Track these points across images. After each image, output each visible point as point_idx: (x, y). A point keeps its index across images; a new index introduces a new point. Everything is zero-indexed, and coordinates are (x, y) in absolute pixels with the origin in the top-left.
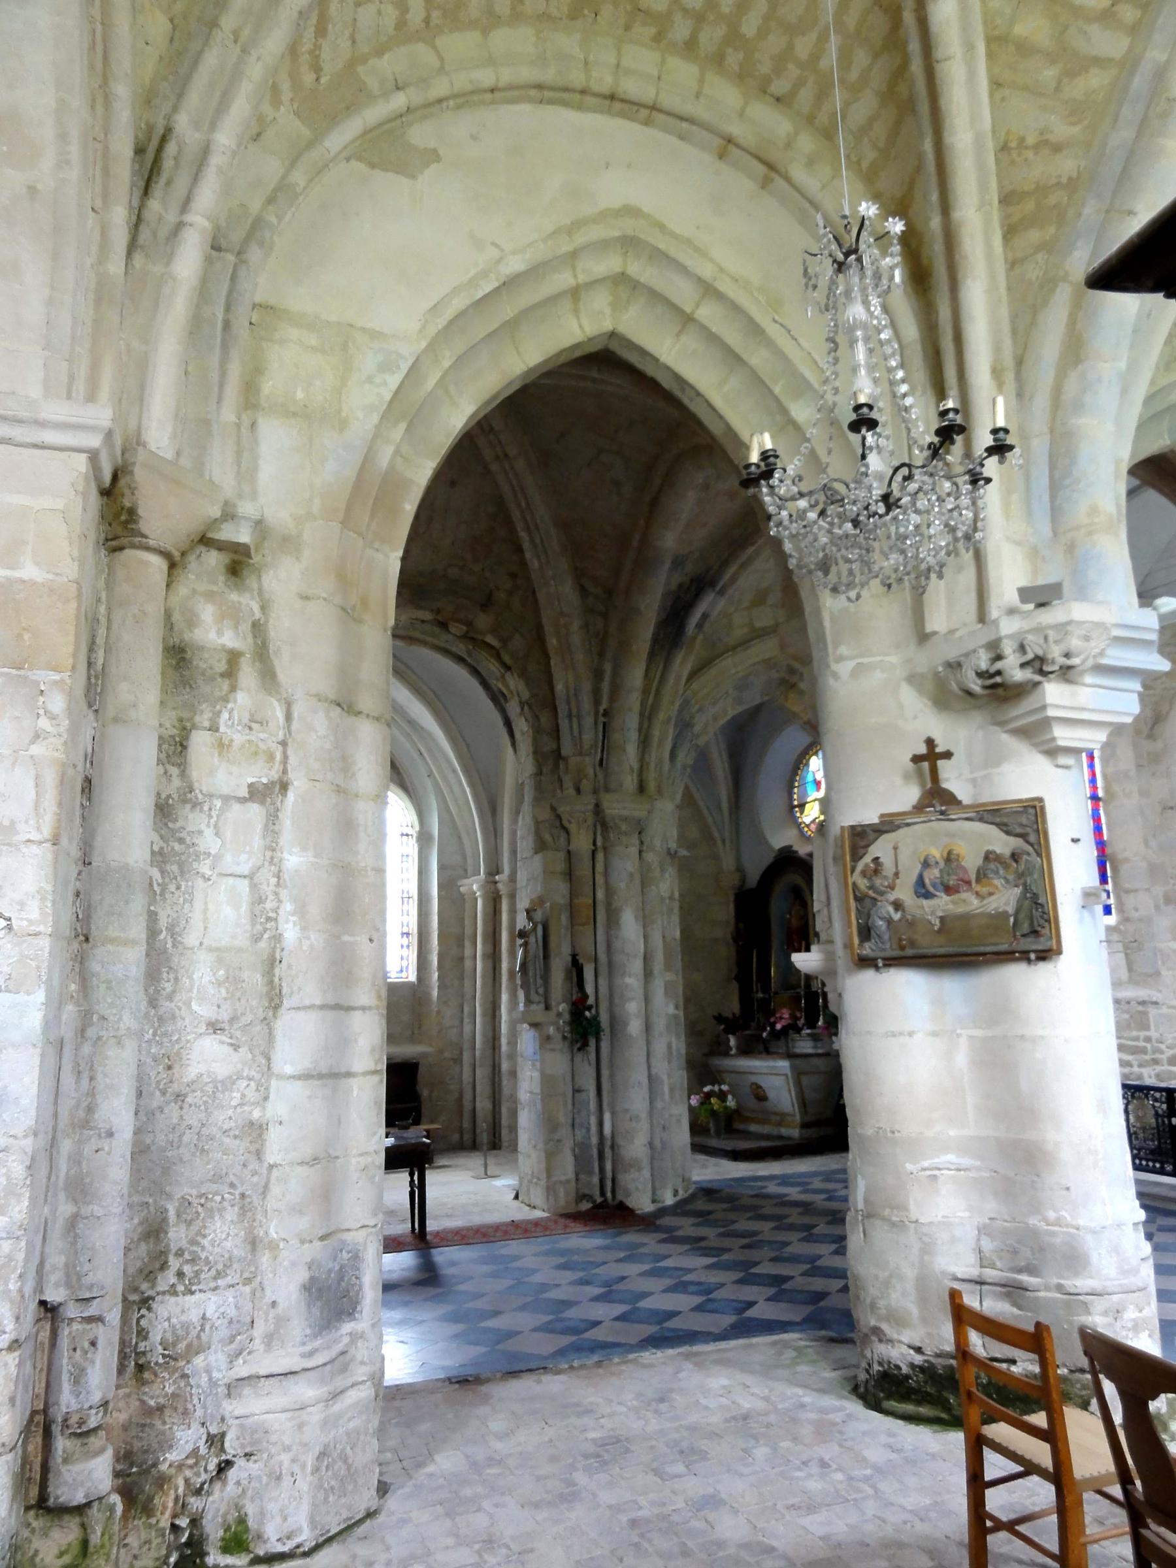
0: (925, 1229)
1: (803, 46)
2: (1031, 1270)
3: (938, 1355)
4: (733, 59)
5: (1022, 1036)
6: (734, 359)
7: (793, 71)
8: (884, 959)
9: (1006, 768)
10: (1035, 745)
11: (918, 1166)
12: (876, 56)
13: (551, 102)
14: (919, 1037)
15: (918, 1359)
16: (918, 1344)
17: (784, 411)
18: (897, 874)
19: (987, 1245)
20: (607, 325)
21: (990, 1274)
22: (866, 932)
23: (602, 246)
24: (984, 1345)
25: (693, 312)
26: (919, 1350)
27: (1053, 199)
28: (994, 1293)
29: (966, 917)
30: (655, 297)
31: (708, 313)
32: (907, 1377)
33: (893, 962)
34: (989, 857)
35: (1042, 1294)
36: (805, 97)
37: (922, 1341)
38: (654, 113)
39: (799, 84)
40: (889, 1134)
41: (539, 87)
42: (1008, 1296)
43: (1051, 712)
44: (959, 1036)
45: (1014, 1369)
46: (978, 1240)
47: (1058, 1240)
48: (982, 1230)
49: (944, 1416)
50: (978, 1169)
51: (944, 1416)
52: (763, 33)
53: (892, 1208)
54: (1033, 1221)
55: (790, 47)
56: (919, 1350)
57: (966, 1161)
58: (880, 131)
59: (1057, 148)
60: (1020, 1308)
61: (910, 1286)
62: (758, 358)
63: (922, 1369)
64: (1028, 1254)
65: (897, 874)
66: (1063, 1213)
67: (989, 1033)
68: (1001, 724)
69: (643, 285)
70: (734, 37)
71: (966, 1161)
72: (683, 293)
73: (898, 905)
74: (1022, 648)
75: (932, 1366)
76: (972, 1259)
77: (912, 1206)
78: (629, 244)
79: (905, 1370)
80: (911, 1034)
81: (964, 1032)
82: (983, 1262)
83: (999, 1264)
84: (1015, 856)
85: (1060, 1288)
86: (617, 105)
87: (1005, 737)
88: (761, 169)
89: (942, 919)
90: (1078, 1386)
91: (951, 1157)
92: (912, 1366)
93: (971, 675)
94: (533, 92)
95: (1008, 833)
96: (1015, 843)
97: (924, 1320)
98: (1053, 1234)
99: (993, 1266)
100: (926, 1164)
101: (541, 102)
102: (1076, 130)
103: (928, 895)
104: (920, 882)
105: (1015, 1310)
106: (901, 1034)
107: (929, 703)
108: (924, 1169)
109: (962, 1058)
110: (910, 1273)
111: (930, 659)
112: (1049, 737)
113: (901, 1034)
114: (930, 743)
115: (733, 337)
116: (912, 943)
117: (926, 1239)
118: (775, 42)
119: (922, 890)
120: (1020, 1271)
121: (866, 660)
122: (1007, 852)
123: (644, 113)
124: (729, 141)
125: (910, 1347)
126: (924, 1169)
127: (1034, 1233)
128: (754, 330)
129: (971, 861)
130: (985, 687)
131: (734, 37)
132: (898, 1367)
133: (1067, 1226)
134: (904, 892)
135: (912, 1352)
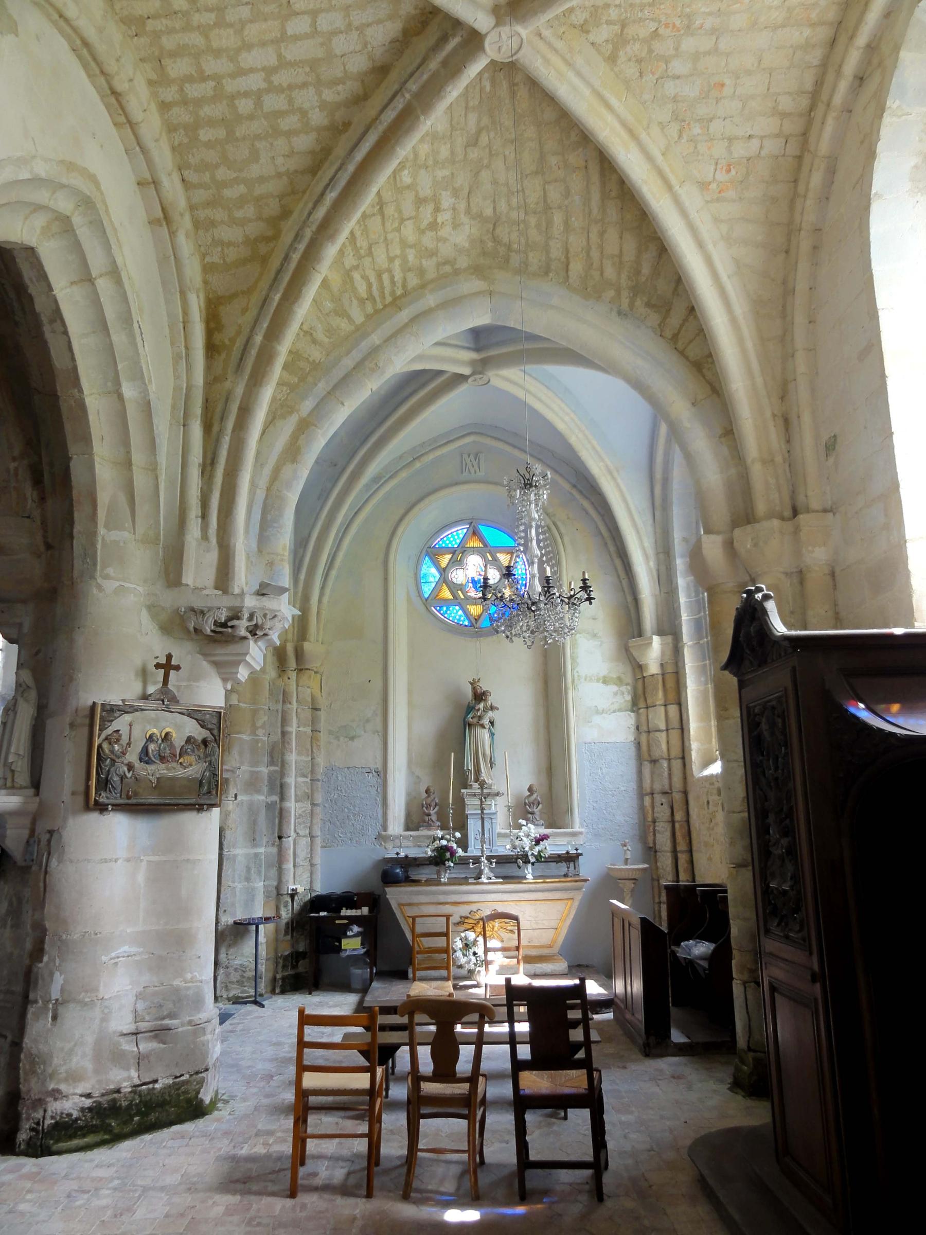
0: (106, 1003)
1: (222, 173)
2: (171, 1016)
3: (103, 1095)
4: (180, 137)
5: (188, 860)
6: (103, 326)
7: (207, 177)
8: (113, 805)
9: (203, 684)
10: (219, 673)
11: (109, 957)
12: (260, 218)
13: (80, 57)
14: (120, 862)
15: (88, 1103)
16: (88, 1092)
17: (118, 383)
18: (129, 744)
19: (140, 1006)
20: (33, 242)
21: (143, 1026)
22: (104, 784)
23: (75, 192)
24: (139, 1076)
25: (95, 279)
26: (88, 1096)
27: (302, 364)
28: (145, 1038)
29: (173, 779)
30: (77, 247)
31: (104, 285)
32: (77, 1119)
33: (118, 808)
34: (189, 740)
35: (180, 1030)
36: (201, 195)
37: (93, 1087)
38: (128, 125)
39: (201, 186)
40: (93, 936)
41: (86, 44)
42: (156, 1037)
43: (248, 658)
44: (141, 861)
45: (157, 1086)
46: (135, 1004)
47: (191, 992)
48: (139, 996)
49: (106, 1137)
50: (140, 954)
51: (106, 1137)
52: (209, 145)
53: (87, 991)
54: (177, 982)
55: (217, 166)
56: (88, 1096)
57: (134, 950)
58: (232, 254)
59: (314, 341)
60: (165, 1044)
61: (89, 1050)
62: (118, 338)
63: (90, 1109)
64: (171, 1006)
65: (129, 744)
66: (196, 973)
67: (164, 858)
68: (205, 655)
69: (75, 235)
70: (192, 129)
71: (134, 950)
72: (97, 262)
73: (130, 767)
74: (251, 618)
75: (99, 1104)
76: (130, 1018)
77: (101, 988)
78: (87, 203)
79: (75, 1114)
80: (116, 861)
81: (145, 859)
82: (137, 1018)
83: (147, 1018)
84: (205, 742)
85: (190, 1023)
86: (113, 100)
87: (205, 663)
88: (160, 214)
89: (158, 778)
90: (195, 1083)
91: (126, 948)
92: (82, 1110)
93: (211, 621)
94: (78, 42)
95: (202, 726)
96: (205, 733)
97: (97, 1071)
98: (188, 988)
99: (143, 1020)
100: (113, 955)
101: (74, 50)
102: (326, 340)
103: (149, 762)
104: (145, 750)
105: (161, 1045)
106: (111, 860)
107: (157, 627)
108: (111, 959)
109: (141, 878)
110: (90, 1039)
111: (170, 600)
112: (234, 671)
113: (111, 860)
114: (169, 657)
115: (110, 313)
116: (136, 794)
117: (106, 1011)
118: (211, 156)
119: (145, 756)
120: (163, 1018)
121: (127, 585)
122: (199, 738)
123: (122, 119)
124: (154, 182)
125: (81, 1096)
126: (111, 959)
127: (177, 990)
128: (127, 319)
129: (178, 741)
130: (212, 631)
131: (192, 129)
132: (69, 1115)
133: (196, 981)
134: (132, 756)
135: (83, 1099)
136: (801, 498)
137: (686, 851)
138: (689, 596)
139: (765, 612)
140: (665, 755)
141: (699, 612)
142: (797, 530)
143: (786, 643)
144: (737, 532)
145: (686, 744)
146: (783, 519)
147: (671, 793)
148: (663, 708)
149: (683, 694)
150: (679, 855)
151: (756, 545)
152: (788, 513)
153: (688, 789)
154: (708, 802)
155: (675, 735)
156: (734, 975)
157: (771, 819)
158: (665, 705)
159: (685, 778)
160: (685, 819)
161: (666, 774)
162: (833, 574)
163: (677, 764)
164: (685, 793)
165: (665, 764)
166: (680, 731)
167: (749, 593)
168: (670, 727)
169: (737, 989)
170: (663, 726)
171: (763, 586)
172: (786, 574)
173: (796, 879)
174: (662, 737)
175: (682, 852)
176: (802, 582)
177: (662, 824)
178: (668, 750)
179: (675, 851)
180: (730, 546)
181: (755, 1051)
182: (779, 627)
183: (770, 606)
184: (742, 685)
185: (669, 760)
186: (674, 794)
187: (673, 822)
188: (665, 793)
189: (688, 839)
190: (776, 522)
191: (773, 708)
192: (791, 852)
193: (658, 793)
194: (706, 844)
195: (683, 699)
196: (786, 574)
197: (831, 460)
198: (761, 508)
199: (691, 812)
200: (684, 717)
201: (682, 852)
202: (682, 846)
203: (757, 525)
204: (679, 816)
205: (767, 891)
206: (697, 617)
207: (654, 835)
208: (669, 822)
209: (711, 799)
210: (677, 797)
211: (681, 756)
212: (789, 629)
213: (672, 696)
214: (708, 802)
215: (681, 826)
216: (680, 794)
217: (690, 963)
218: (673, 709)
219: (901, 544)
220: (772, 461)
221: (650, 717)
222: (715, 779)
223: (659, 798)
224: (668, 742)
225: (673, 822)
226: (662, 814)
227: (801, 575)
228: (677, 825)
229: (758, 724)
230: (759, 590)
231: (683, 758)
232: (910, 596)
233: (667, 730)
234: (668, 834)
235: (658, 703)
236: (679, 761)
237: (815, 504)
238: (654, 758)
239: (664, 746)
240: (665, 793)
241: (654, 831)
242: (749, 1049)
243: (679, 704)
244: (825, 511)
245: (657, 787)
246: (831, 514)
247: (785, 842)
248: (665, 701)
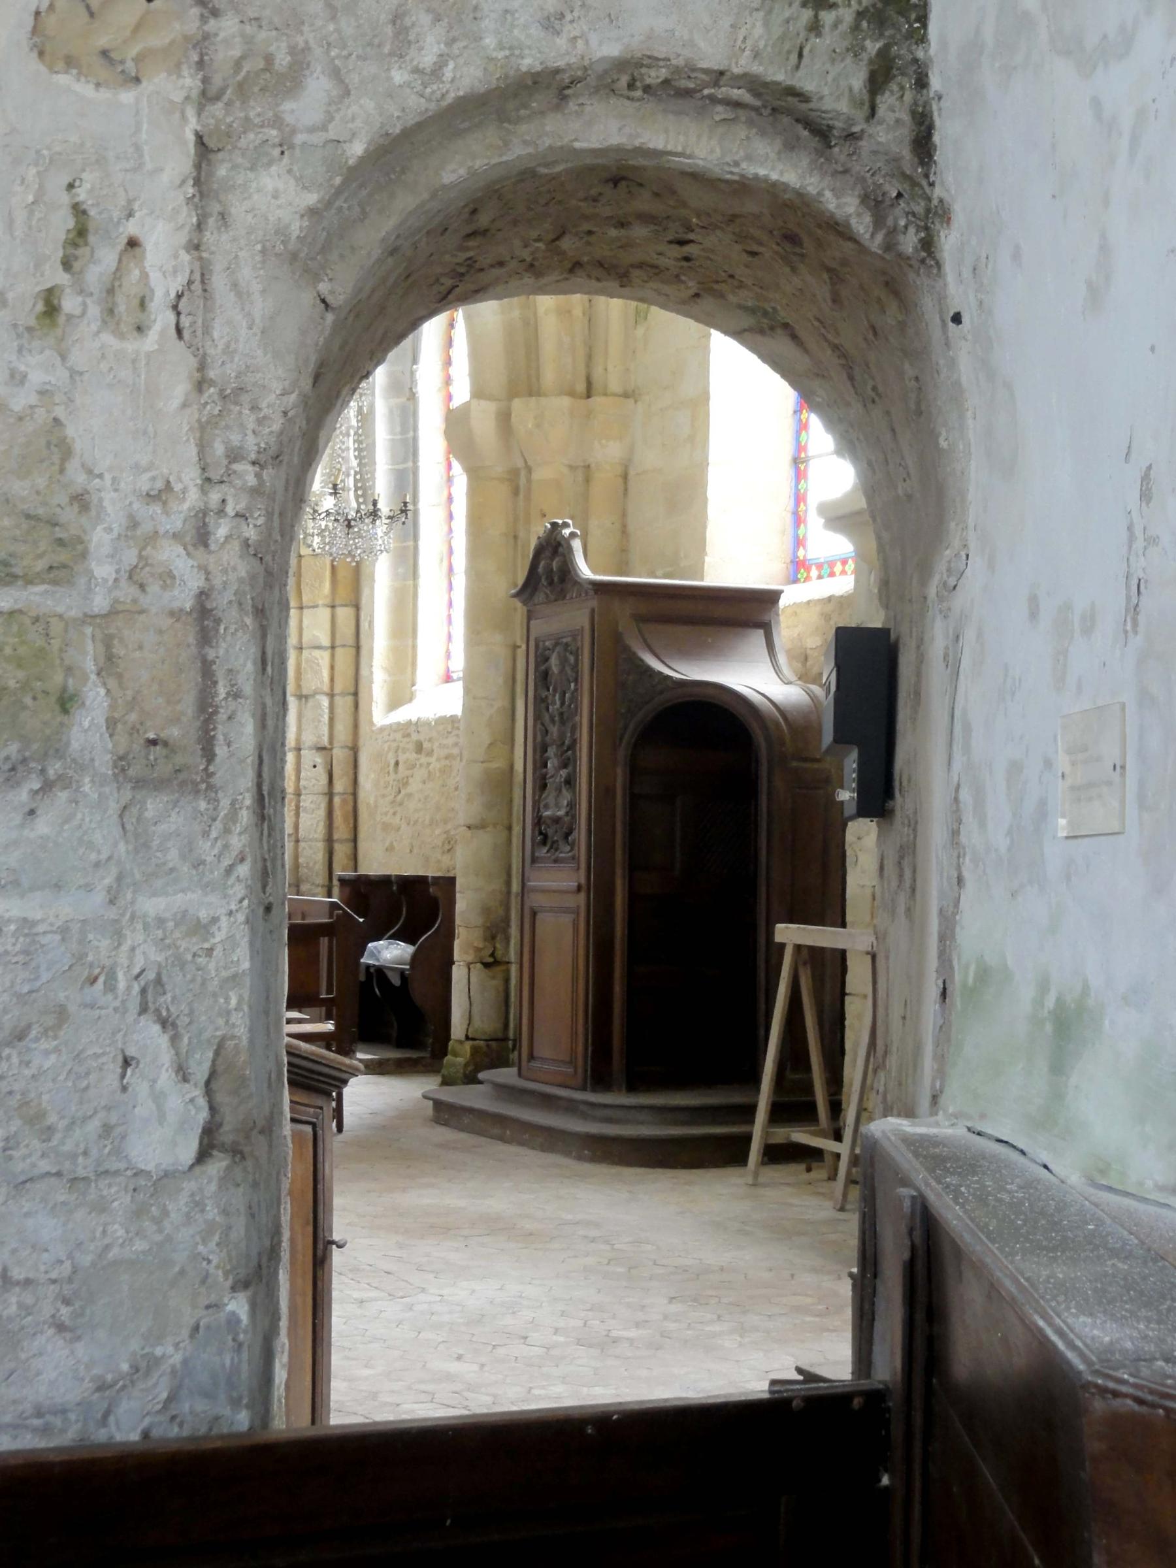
136: (598, 373)
137: (347, 840)
138: (392, 431)
139: (570, 549)
140: (326, 688)
141: (405, 460)
142: (589, 415)
143: (586, 586)
144: (517, 404)
145: (364, 672)
146: (572, 394)
147: (331, 749)
148: (327, 612)
149: (365, 593)
150: (337, 846)
151: (538, 426)
152: (581, 387)
153: (361, 742)
154: (397, 763)
155: (344, 656)
156: (456, 957)
157: (551, 751)
158: (333, 607)
159: (356, 726)
160: (350, 790)
161: (326, 718)
162: (625, 477)
163: (344, 704)
164: (355, 750)
165: (325, 702)
166: (353, 651)
167: (554, 525)
168: (338, 643)
169: (458, 973)
170: (325, 641)
171: (570, 522)
172: (572, 468)
173: (572, 805)
174: (324, 658)
175: (339, 841)
176: (587, 480)
177: (310, 798)
178: (332, 680)
179: (330, 840)
180: (505, 419)
181: (473, 1039)
182: (585, 571)
183: (577, 544)
184: (530, 616)
185: (331, 696)
186: (335, 751)
187: (330, 795)
188: (322, 749)
189: (352, 821)
190: (566, 401)
191: (567, 645)
192: (570, 782)
193: (310, 748)
194: (386, 827)
195: (364, 601)
196: (572, 468)
197: (640, 331)
198: (549, 376)
199: (362, 779)
200: (364, 625)
201: (341, 841)
202: (342, 831)
203: (543, 400)
204: (339, 786)
205: (538, 821)
206: (401, 467)
207: (297, 815)
208: (326, 794)
209: (402, 758)
210: (340, 754)
211: (352, 690)
212: (594, 571)
213: (343, 593)
214: (397, 763)
215: (344, 801)
216: (347, 750)
217: (379, 973)
218: (345, 614)
219: (703, 465)
220: (569, 312)
221: (305, 622)
222: (413, 728)
223: (309, 756)
224: (332, 668)
225: (330, 795)
226: (314, 781)
227: (587, 471)
228: (337, 800)
229: (547, 659)
230: (566, 525)
231: (356, 694)
232: (705, 527)
233: (333, 647)
234: (322, 812)
235: (320, 602)
236: (350, 699)
237: (615, 386)
238: (305, 692)
239: (326, 674)
240: (322, 749)
241: (298, 807)
242: (467, 1038)
243: (357, 607)
244: (626, 395)
245: (309, 739)
246: (631, 401)
247: (564, 773)
248: (333, 600)
